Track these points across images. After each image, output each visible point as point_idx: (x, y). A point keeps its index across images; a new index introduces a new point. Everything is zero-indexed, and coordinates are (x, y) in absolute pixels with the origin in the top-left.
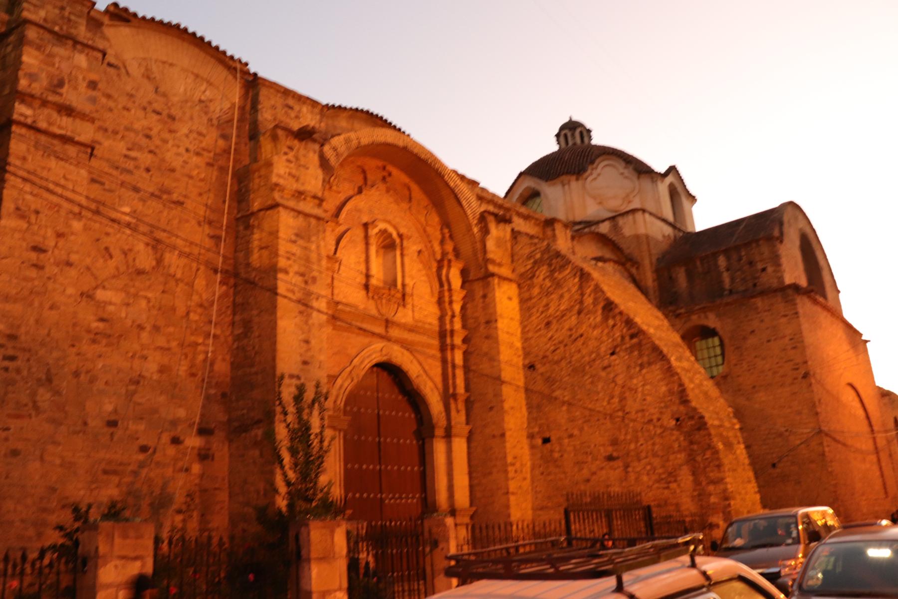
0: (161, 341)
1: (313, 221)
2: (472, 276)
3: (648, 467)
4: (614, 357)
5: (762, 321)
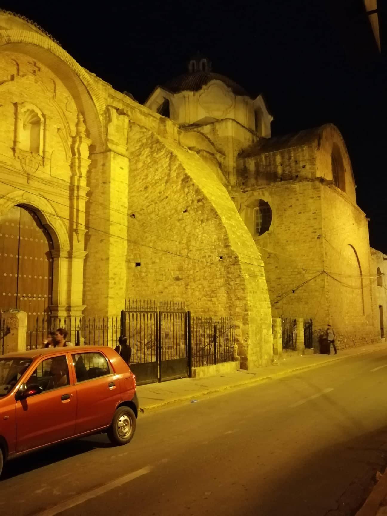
2: (97, 150)
3: (200, 287)
4: (186, 213)
5: (297, 200)
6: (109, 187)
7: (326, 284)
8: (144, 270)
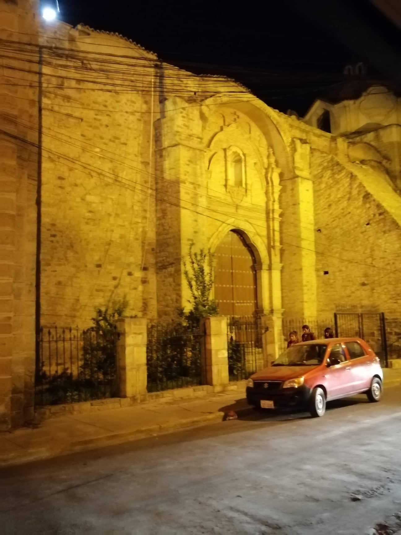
0: (120, 222)
1: (198, 152)
2: (286, 176)
3: (386, 290)
4: (368, 226)
6: (299, 208)
8: (332, 277)
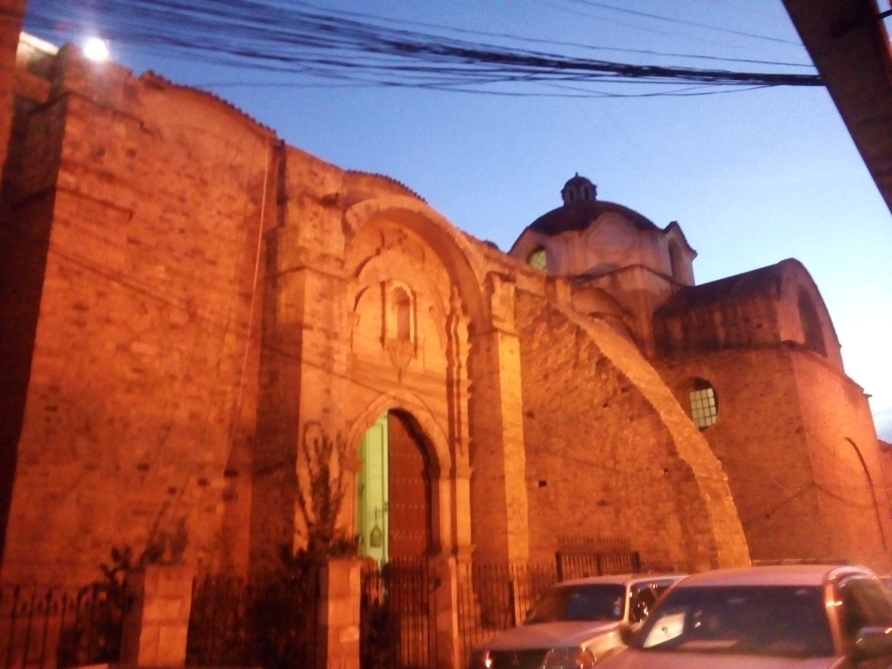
0: (192, 389)
1: (336, 283)
2: (478, 329)
4: (606, 409)
7: (820, 503)
8: (552, 490)
